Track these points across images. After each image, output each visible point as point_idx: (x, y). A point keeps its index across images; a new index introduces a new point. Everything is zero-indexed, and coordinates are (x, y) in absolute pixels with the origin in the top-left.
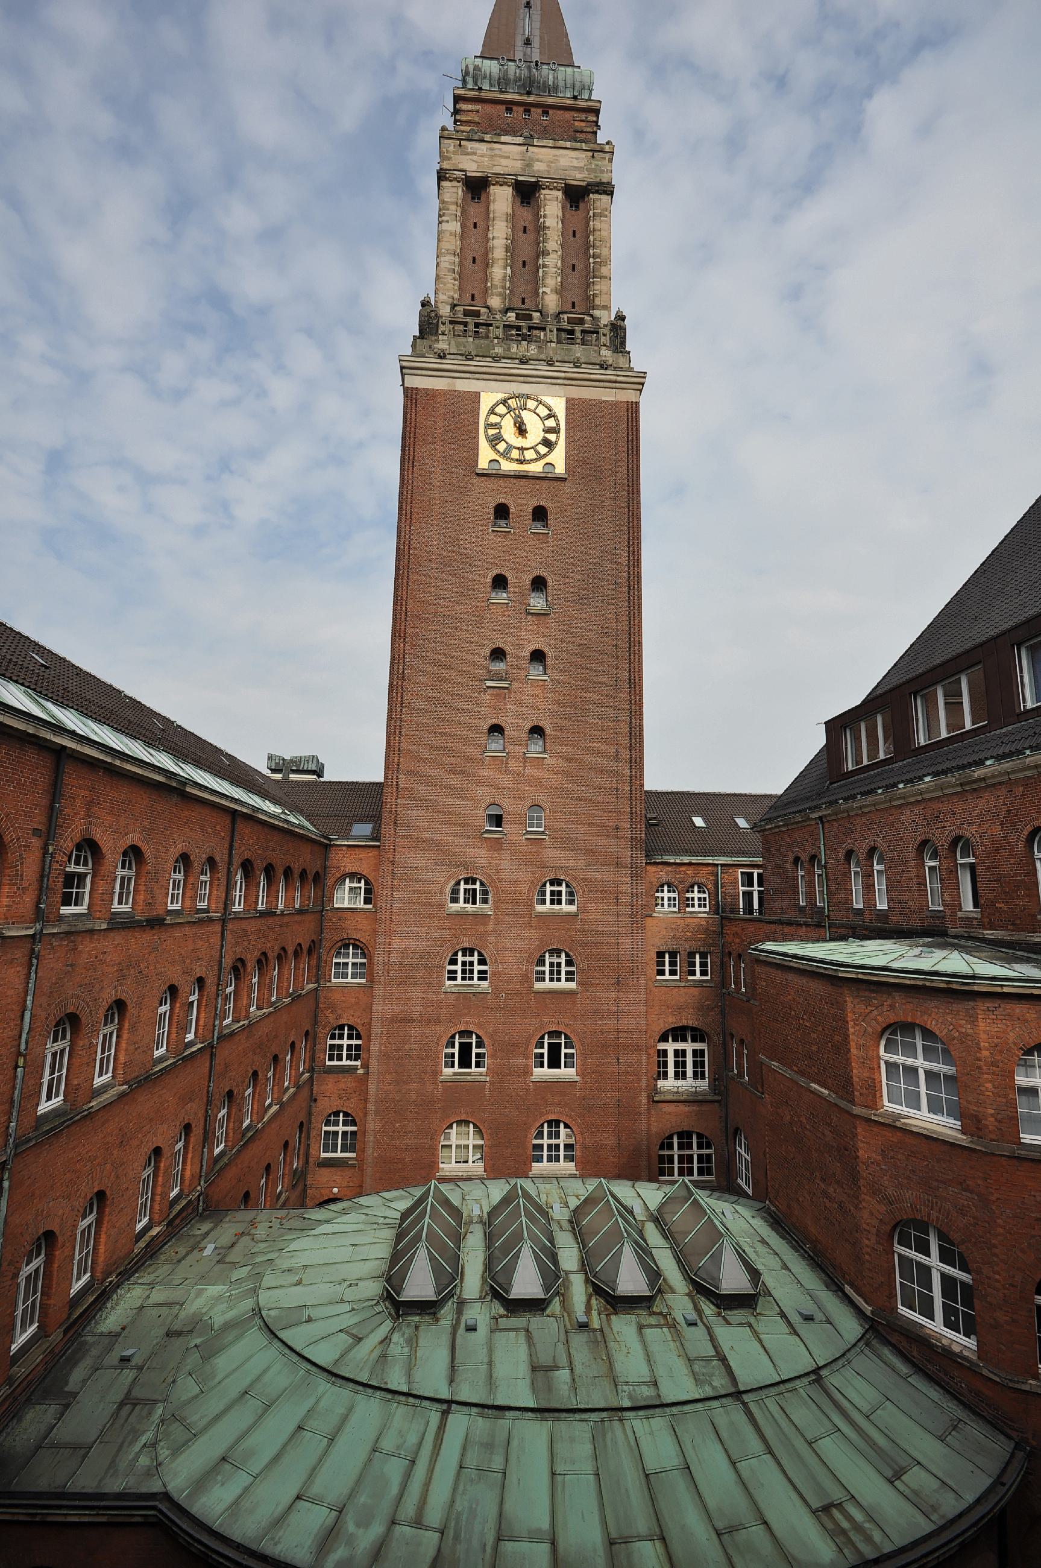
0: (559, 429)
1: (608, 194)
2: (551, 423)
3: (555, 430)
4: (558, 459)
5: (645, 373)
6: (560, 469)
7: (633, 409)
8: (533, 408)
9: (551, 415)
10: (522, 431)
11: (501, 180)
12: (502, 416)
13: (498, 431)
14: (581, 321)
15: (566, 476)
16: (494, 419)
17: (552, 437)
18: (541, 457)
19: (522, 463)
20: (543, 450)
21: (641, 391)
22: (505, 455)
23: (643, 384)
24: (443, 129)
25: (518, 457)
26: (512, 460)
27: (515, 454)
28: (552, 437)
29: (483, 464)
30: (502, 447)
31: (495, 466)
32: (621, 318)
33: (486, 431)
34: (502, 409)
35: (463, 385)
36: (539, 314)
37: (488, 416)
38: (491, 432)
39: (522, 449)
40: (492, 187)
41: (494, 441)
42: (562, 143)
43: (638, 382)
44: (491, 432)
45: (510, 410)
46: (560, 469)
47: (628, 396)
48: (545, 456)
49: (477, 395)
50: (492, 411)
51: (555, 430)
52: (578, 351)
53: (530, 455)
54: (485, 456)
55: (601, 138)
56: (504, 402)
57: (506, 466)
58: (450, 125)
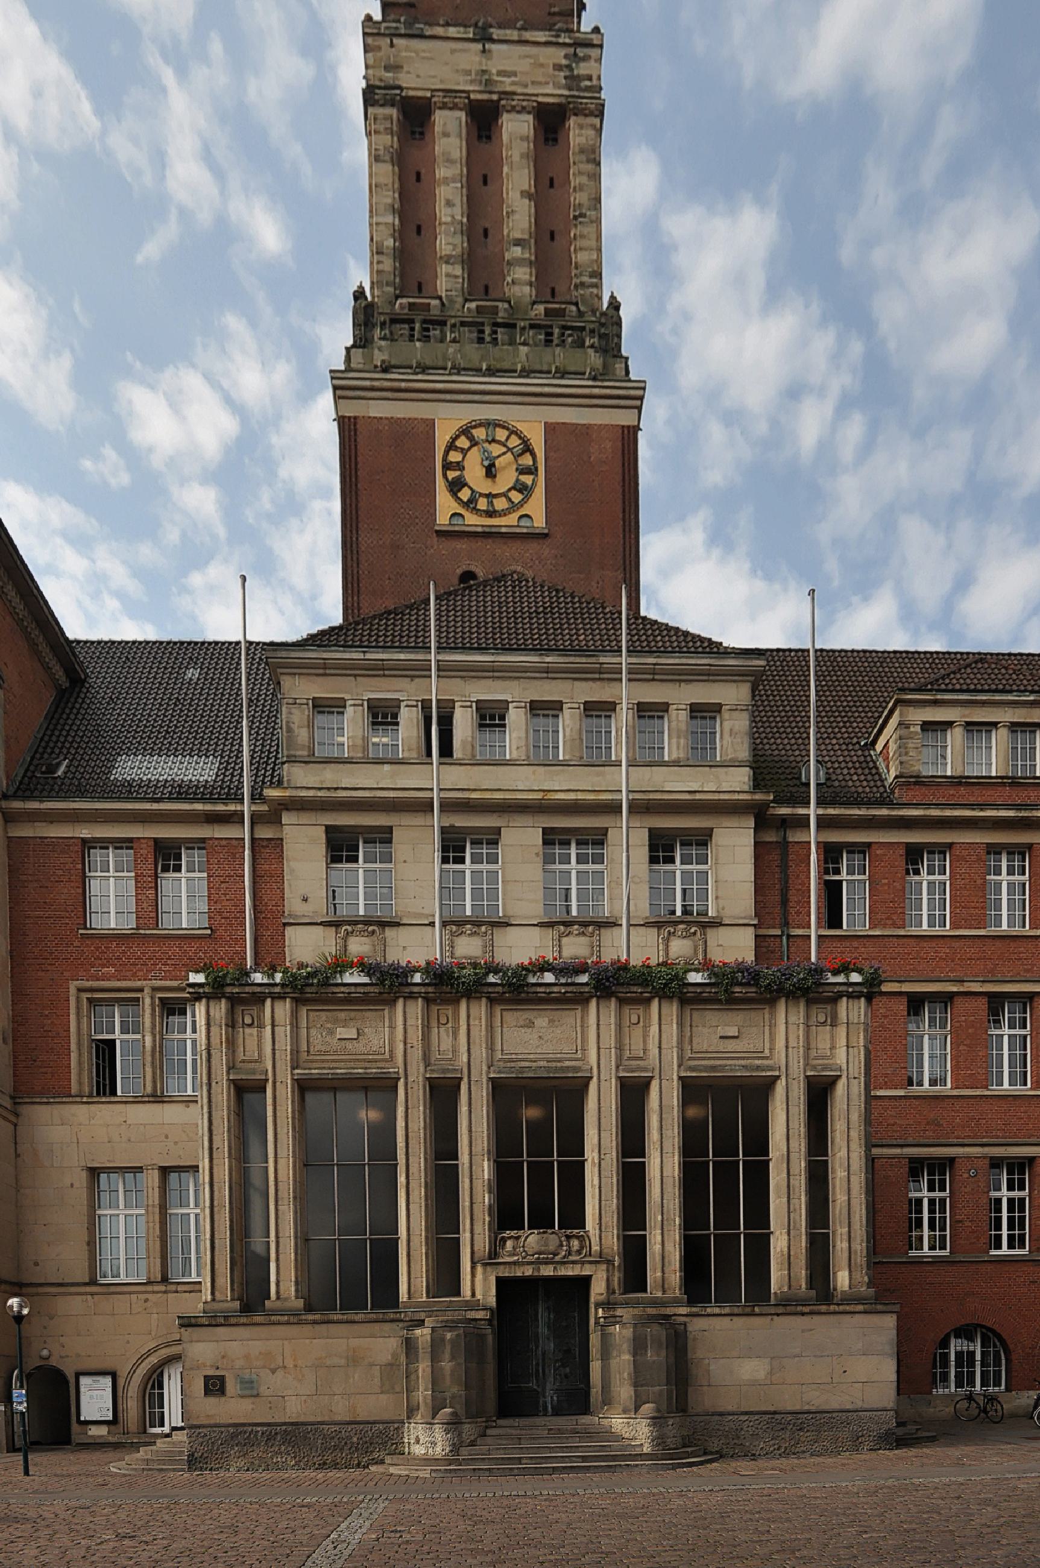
0: (536, 469)
1: (596, 116)
2: (527, 460)
3: (532, 471)
4: (537, 510)
5: (644, 382)
6: (540, 522)
7: (629, 436)
8: (503, 439)
10: (490, 472)
11: (451, 98)
12: (464, 452)
13: (458, 473)
14: (561, 313)
15: (546, 531)
16: (455, 457)
17: (527, 479)
18: (514, 507)
19: (491, 516)
20: (516, 497)
21: (639, 409)
22: (470, 504)
23: (641, 398)
24: (369, 18)
25: (485, 508)
26: (476, 511)
27: (482, 504)
28: (527, 479)
29: (442, 519)
30: (465, 494)
31: (456, 521)
32: (615, 305)
33: (445, 476)
34: (462, 442)
36: (506, 305)
37: (446, 453)
38: (451, 475)
39: (490, 496)
40: (438, 112)
41: (456, 486)
42: (528, 35)
43: (635, 399)
44: (451, 475)
45: (474, 443)
46: (540, 522)
47: (624, 418)
48: (522, 504)
49: (431, 424)
50: (451, 446)
51: (532, 471)
52: (559, 356)
53: (500, 504)
54: (445, 506)
55: (586, 26)
56: (465, 431)
57: (472, 520)
58: (377, 16)
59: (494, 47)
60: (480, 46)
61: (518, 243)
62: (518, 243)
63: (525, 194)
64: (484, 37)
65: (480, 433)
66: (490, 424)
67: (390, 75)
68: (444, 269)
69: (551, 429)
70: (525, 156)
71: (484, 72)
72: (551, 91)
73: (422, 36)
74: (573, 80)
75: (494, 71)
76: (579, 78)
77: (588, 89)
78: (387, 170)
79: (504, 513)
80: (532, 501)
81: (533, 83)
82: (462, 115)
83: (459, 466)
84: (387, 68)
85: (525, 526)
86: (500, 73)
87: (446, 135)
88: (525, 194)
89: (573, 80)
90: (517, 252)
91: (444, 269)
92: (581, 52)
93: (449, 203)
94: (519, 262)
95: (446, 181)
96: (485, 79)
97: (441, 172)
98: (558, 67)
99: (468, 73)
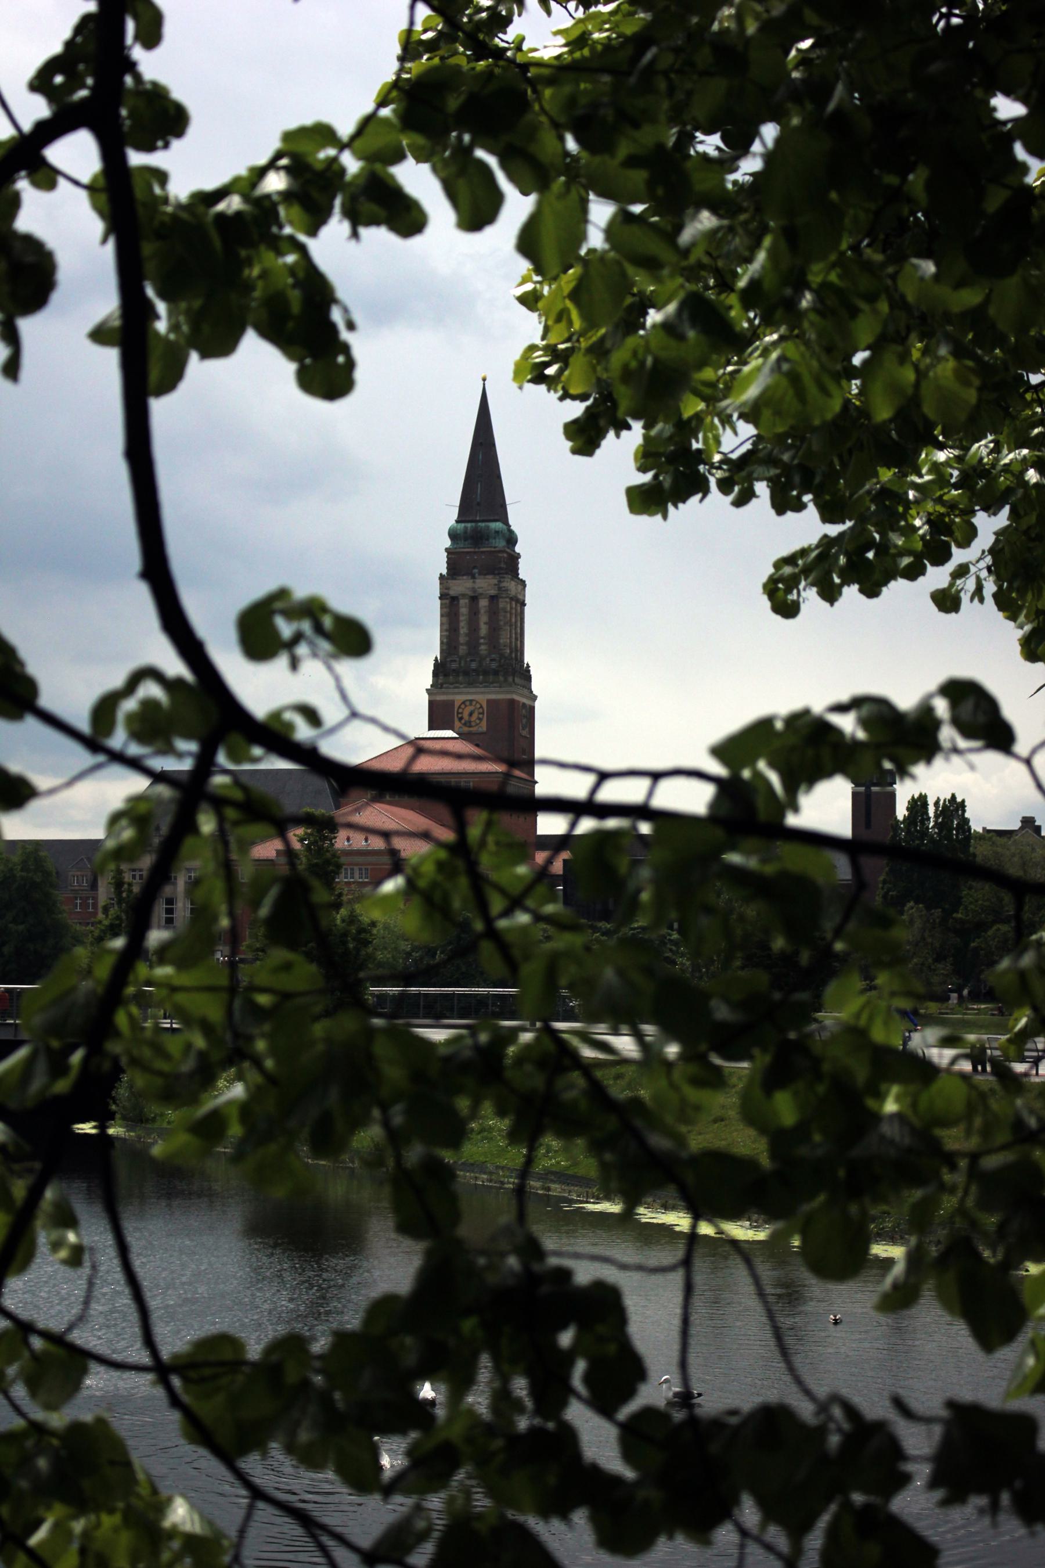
2: (481, 710)
4: (484, 723)
9: (481, 707)
10: (471, 714)
11: (464, 595)
16: (460, 711)
17: (481, 716)
18: (477, 724)
20: (478, 721)
22: (465, 724)
24: (441, 574)
27: (468, 724)
28: (481, 716)
30: (463, 721)
35: (450, 697)
38: (460, 716)
41: (461, 719)
46: (485, 729)
50: (459, 707)
56: (464, 703)
59: (478, 581)
60: (472, 581)
61: (482, 638)
62: (482, 638)
63: (485, 623)
64: (473, 577)
65: (468, 703)
66: (471, 701)
67: (446, 591)
68: (461, 647)
69: (489, 701)
70: (485, 612)
71: (473, 588)
72: (493, 592)
73: (455, 579)
74: (500, 589)
75: (476, 587)
76: (501, 588)
77: (504, 591)
78: (445, 619)
79: (475, 726)
80: (482, 723)
81: (488, 590)
82: (467, 601)
83: (462, 713)
84: (446, 589)
85: (480, 730)
86: (479, 588)
87: (462, 607)
88: (485, 623)
89: (500, 589)
90: (482, 641)
91: (461, 647)
92: (502, 580)
93: (463, 628)
94: (483, 644)
95: (462, 621)
96: (474, 590)
97: (462, 618)
98: (495, 585)
99: (469, 588)
